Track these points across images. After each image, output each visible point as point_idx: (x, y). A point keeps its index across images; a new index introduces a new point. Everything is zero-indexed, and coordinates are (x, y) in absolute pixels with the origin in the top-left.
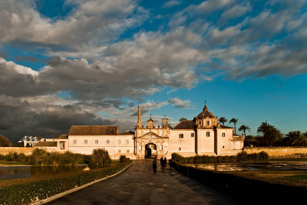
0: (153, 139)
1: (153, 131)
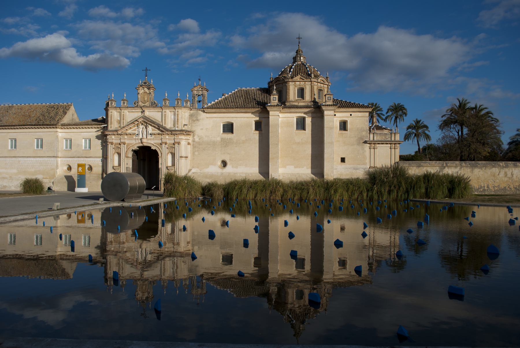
0: (149, 137)
1: (150, 113)
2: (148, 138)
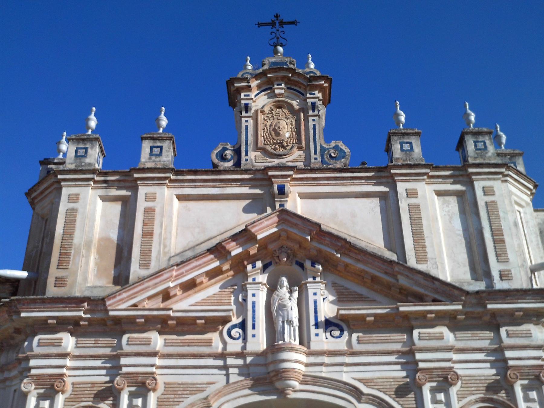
2: (315, 346)
